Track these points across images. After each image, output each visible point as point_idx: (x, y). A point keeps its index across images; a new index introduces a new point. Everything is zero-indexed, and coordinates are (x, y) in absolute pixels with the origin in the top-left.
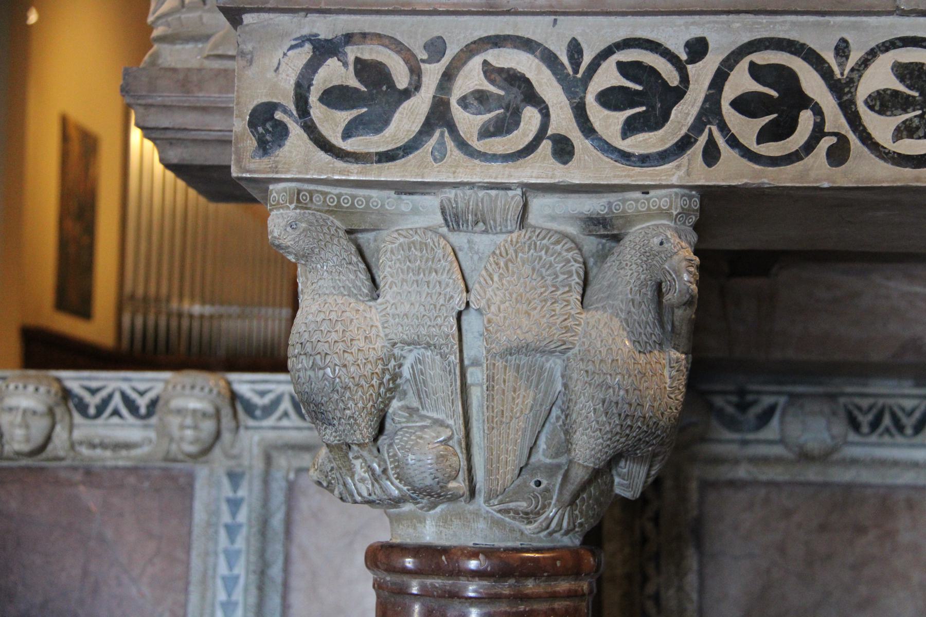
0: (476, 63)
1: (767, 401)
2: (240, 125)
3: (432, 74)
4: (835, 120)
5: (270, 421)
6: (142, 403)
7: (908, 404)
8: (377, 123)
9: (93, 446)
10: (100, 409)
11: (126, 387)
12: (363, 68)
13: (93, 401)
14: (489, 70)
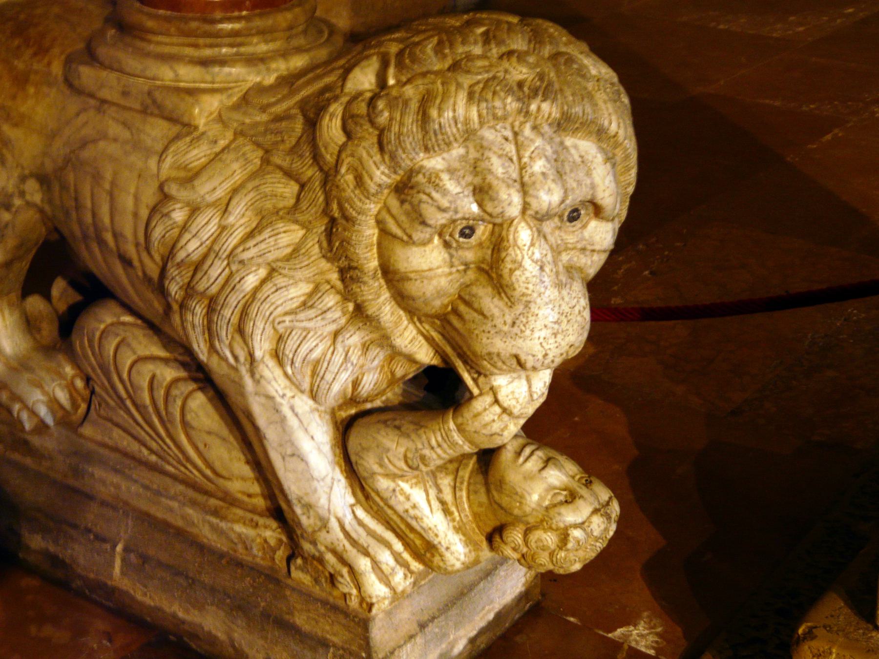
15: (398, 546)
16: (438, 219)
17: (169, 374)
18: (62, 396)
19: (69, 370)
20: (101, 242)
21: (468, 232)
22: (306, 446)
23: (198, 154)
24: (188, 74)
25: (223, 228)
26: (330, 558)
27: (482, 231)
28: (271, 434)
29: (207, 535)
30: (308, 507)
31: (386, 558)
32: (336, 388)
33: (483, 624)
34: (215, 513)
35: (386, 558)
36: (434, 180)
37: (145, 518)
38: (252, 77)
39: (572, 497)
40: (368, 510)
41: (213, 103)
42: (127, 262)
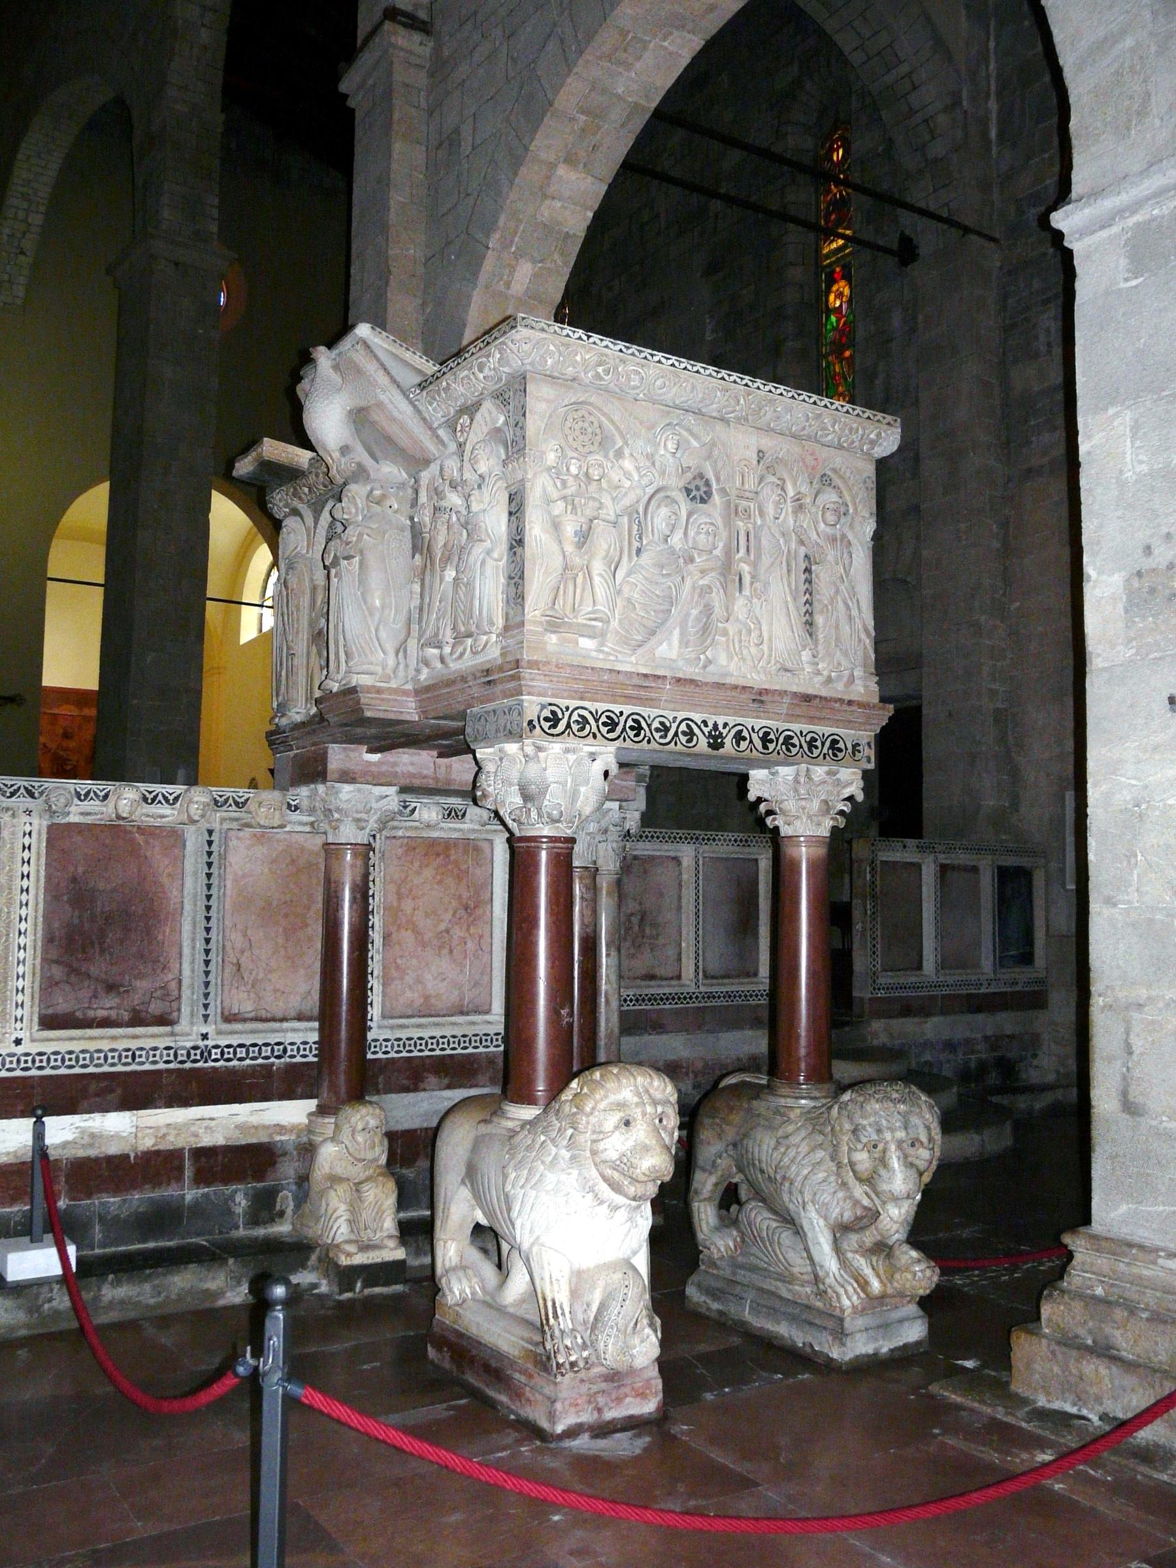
0: (576, 713)
1: (413, 805)
2: (525, 724)
3: (567, 714)
4: (648, 734)
5: (224, 808)
6: (171, 798)
7: (460, 807)
8: (554, 726)
9: (148, 816)
10: (153, 800)
11: (164, 791)
12: (553, 713)
13: (150, 797)
14: (579, 716)
15: (856, 1285)
16: (864, 1140)
17: (774, 1224)
18: (731, 1244)
19: (735, 1233)
20: (754, 1165)
21: (875, 1146)
22: (822, 1240)
23: (790, 1128)
24: (790, 1102)
25: (797, 1153)
26: (829, 1290)
27: (881, 1147)
28: (809, 1235)
29: (785, 1294)
30: (822, 1267)
31: (850, 1289)
32: (834, 1215)
33: (897, 1345)
34: (789, 1283)
35: (850, 1289)
36: (864, 1128)
37: (761, 1290)
38: (812, 1104)
39: (919, 1261)
40: (846, 1272)
41: (798, 1111)
42: (762, 1171)
